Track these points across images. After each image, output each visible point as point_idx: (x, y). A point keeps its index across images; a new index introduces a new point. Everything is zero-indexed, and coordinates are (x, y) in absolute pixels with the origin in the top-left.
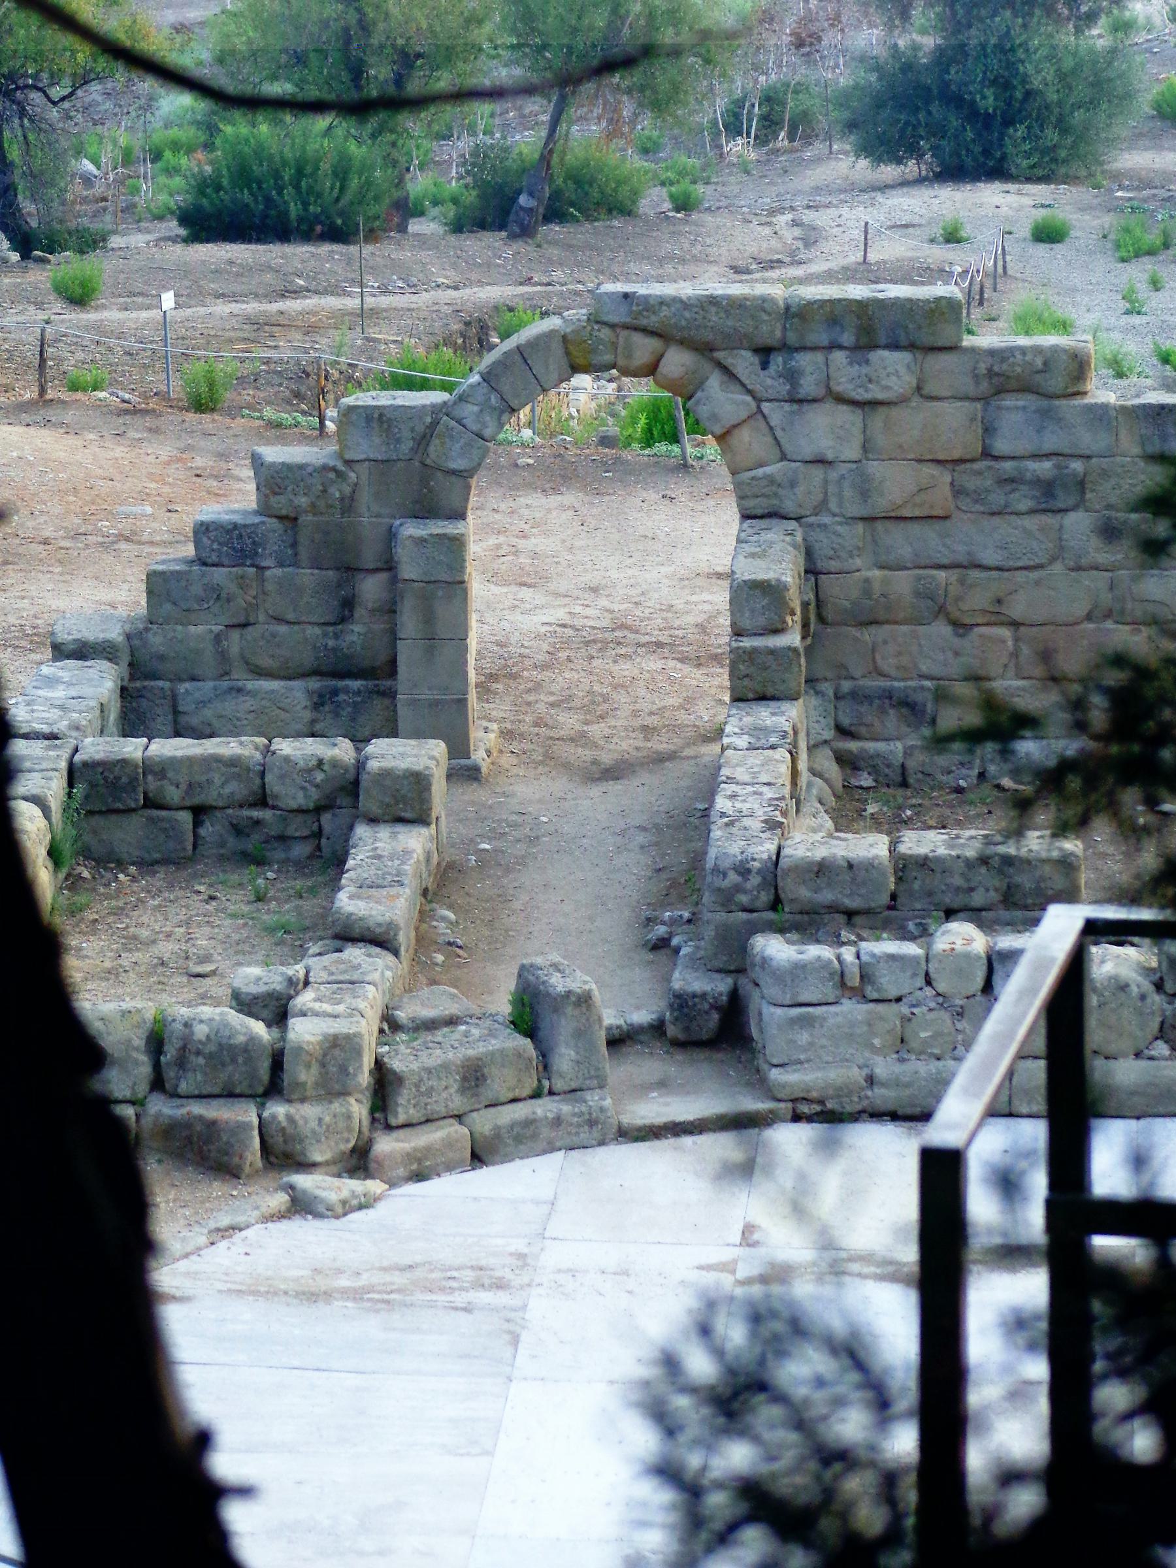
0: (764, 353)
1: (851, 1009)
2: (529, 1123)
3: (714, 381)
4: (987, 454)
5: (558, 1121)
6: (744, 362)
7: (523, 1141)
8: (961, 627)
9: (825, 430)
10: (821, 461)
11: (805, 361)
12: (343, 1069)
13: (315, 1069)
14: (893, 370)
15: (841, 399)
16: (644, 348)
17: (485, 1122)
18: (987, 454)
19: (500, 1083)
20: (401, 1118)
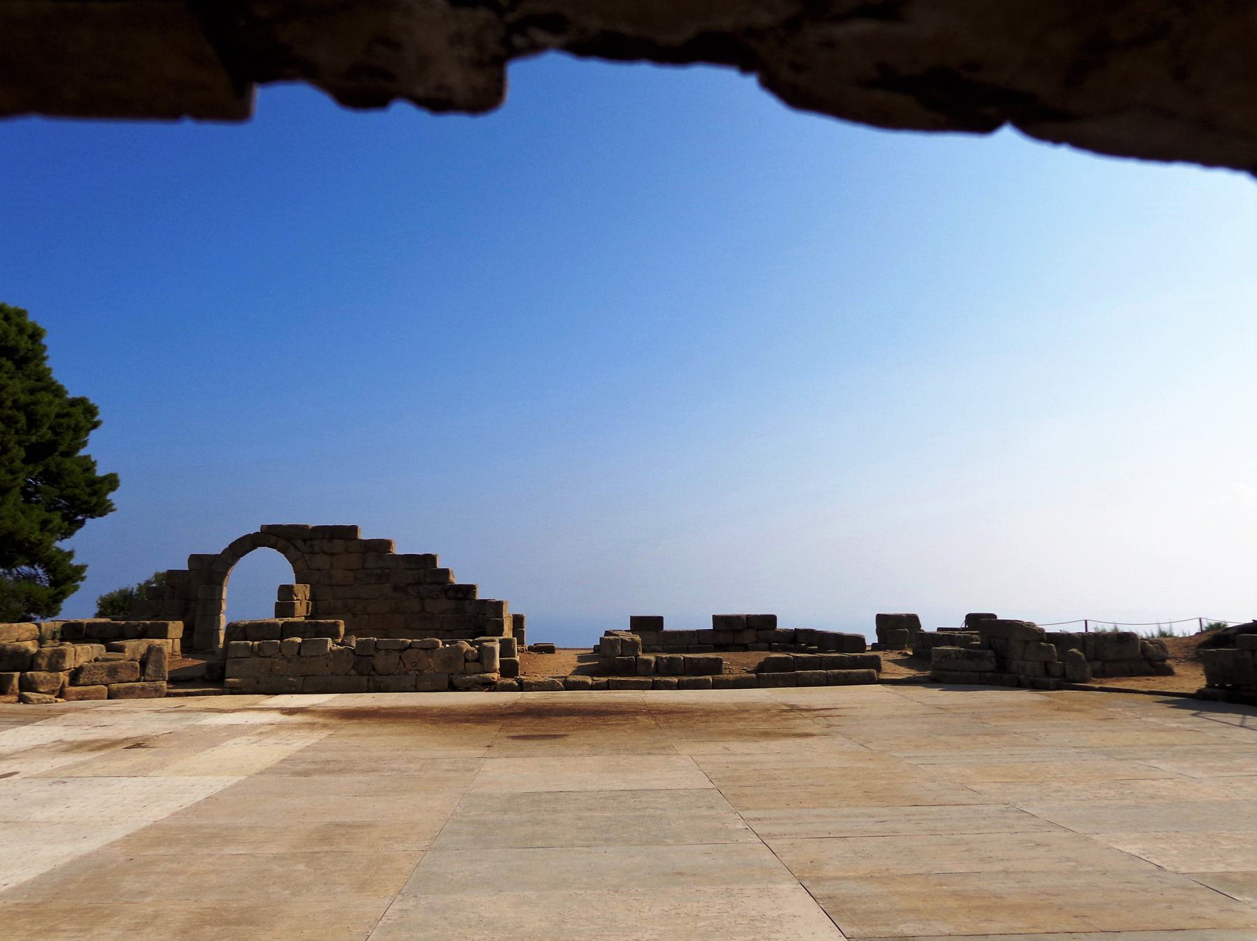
0: (305, 541)
1: (256, 660)
2: (131, 688)
3: (292, 549)
4: (363, 568)
5: (143, 688)
6: (299, 543)
7: (129, 693)
8: (355, 615)
9: (321, 561)
10: (318, 570)
11: (316, 542)
12: (58, 662)
13: (46, 660)
14: (339, 545)
15: (325, 553)
16: (273, 539)
17: (114, 686)
18: (363, 568)
19: (123, 675)
20: (81, 682)
